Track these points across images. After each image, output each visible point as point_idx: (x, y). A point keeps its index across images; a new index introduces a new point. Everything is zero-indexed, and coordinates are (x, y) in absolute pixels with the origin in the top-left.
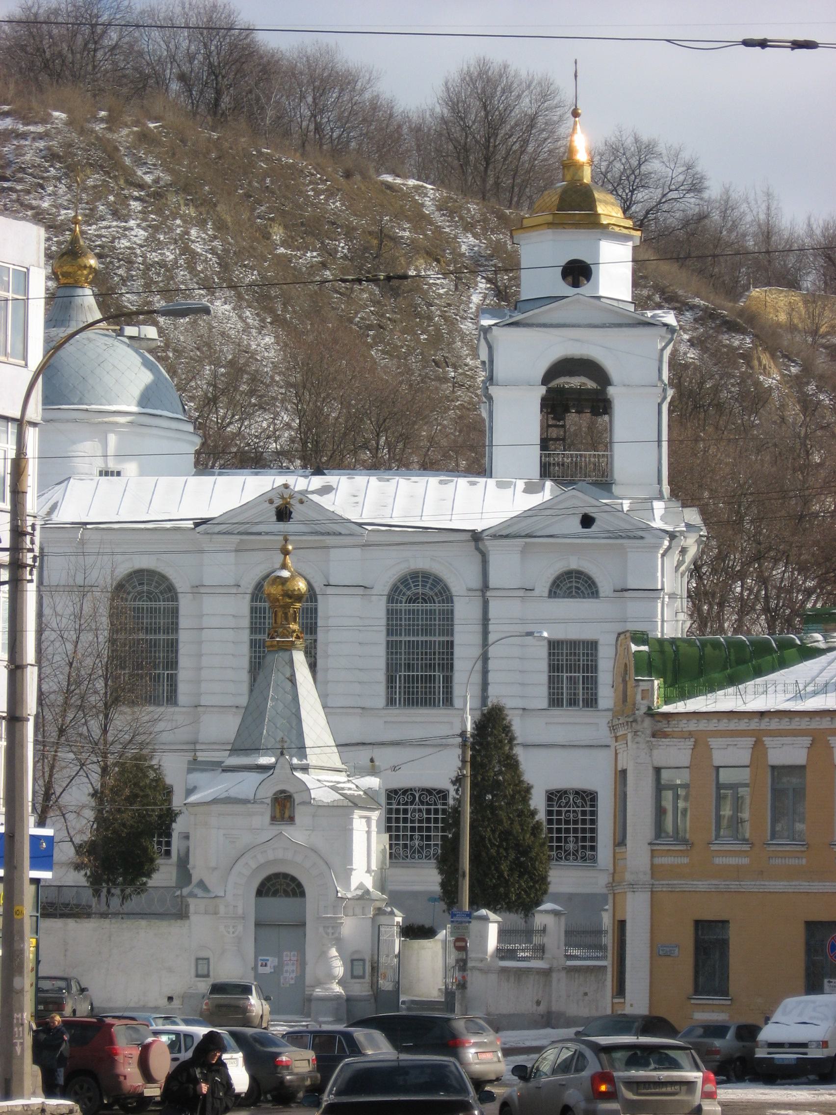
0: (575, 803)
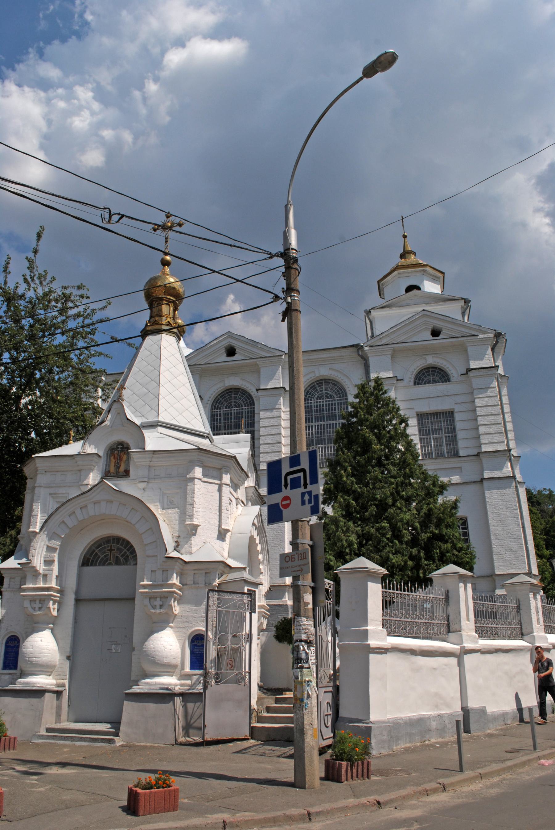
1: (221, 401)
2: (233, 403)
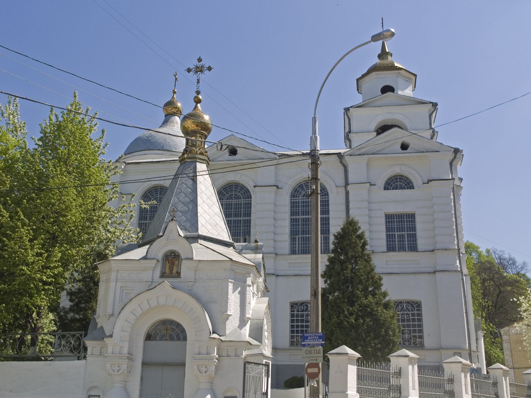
0: (408, 309)
1: (223, 193)
2: (233, 196)
